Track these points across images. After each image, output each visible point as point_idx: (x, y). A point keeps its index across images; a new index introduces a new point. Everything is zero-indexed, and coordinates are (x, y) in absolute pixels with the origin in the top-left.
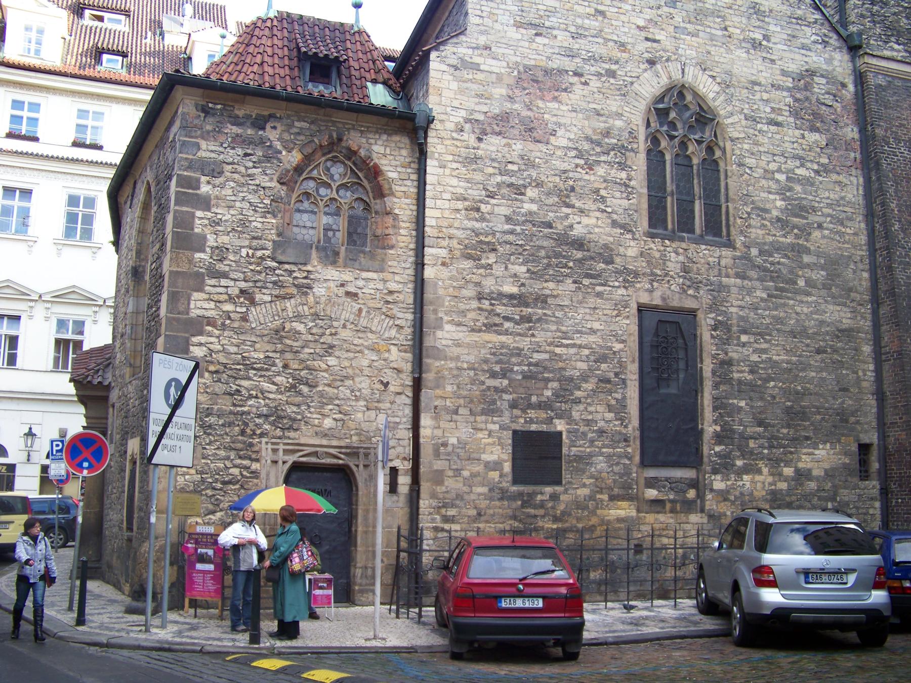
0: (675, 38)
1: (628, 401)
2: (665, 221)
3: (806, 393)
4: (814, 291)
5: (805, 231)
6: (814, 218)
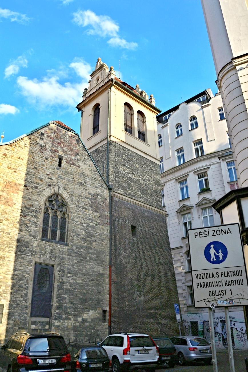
0: (58, 179)
1: (28, 294)
2: (47, 235)
3: (88, 293)
4: (92, 261)
5: (91, 242)
6: (94, 239)
